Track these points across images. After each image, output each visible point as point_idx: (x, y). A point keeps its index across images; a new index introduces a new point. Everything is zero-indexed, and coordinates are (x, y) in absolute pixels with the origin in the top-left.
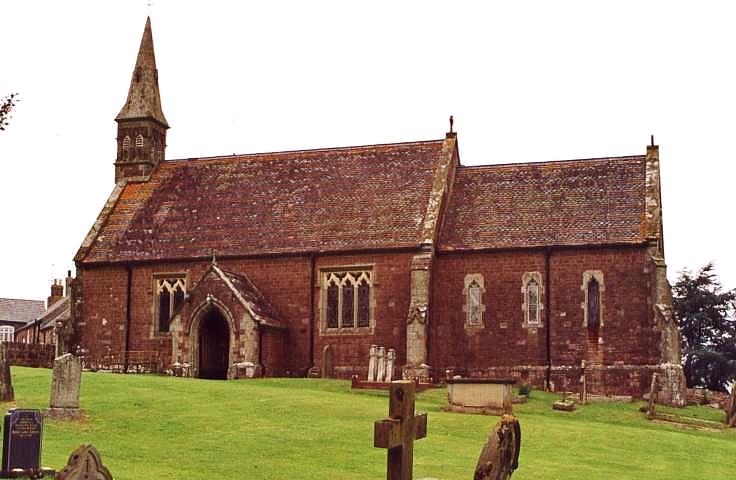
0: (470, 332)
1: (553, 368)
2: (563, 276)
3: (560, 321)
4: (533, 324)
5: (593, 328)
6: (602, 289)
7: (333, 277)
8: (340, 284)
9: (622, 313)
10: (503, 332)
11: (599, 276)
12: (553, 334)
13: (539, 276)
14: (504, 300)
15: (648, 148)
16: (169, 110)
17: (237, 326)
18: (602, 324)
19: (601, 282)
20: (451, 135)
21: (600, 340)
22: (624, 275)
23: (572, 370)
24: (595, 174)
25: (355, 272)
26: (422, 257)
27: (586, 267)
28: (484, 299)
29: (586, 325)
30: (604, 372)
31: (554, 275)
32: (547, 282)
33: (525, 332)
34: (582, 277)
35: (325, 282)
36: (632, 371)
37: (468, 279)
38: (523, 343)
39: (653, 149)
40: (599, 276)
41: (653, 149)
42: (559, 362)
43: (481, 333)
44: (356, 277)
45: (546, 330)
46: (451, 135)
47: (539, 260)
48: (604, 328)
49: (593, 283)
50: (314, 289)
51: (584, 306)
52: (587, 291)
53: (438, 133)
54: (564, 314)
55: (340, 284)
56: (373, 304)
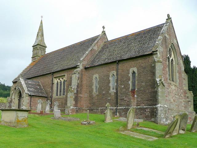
0: (94, 95)
1: (118, 108)
2: (123, 71)
3: (121, 89)
4: (112, 91)
5: (133, 91)
6: (137, 75)
7: (58, 79)
8: (59, 81)
9: (144, 84)
10: (104, 94)
11: (135, 70)
12: (119, 94)
13: (115, 73)
14: (104, 82)
15: (167, 19)
16: (47, 42)
17: (23, 96)
18: (136, 89)
19: (136, 72)
20: (104, 32)
21: (136, 96)
22: (145, 68)
23: (125, 108)
24: (144, 33)
25: (59, 78)
26: (77, 70)
27: (131, 67)
28: (100, 82)
29: (130, 90)
30: (137, 109)
31: (120, 71)
32: (117, 74)
33: (110, 94)
34: (129, 71)
35: (55, 81)
36: (147, 108)
37: (94, 77)
38: (110, 98)
39: (169, 18)
40: (135, 70)
41: (169, 18)
42: (121, 105)
43: (97, 96)
44: (59, 79)
45: (116, 93)
46: (104, 32)
47: (114, 66)
48: (137, 91)
49: (134, 73)
50: (53, 84)
51: (130, 83)
52: (131, 77)
53: (99, 32)
54: (123, 86)
55: (59, 81)
56: (66, 87)
